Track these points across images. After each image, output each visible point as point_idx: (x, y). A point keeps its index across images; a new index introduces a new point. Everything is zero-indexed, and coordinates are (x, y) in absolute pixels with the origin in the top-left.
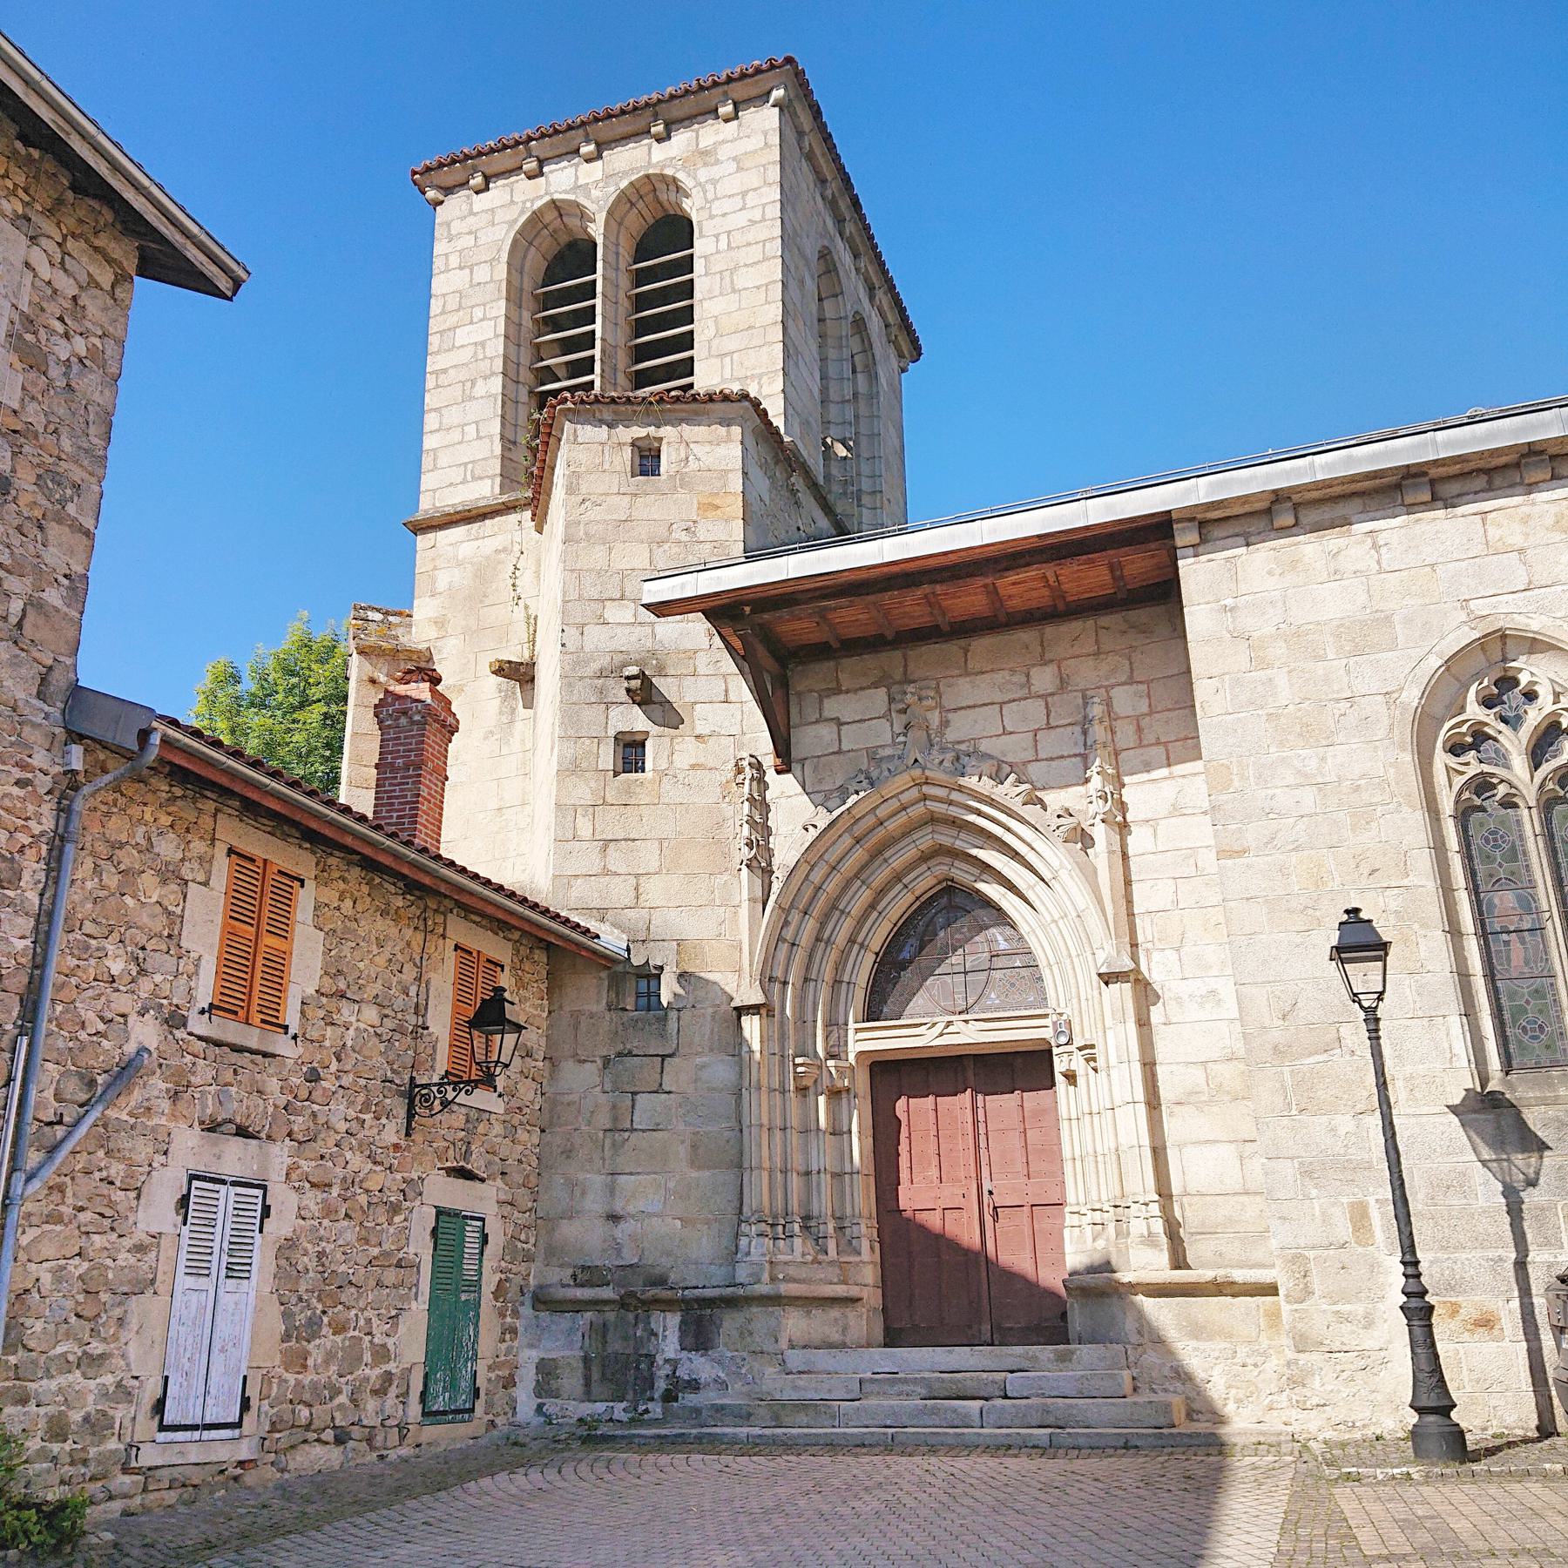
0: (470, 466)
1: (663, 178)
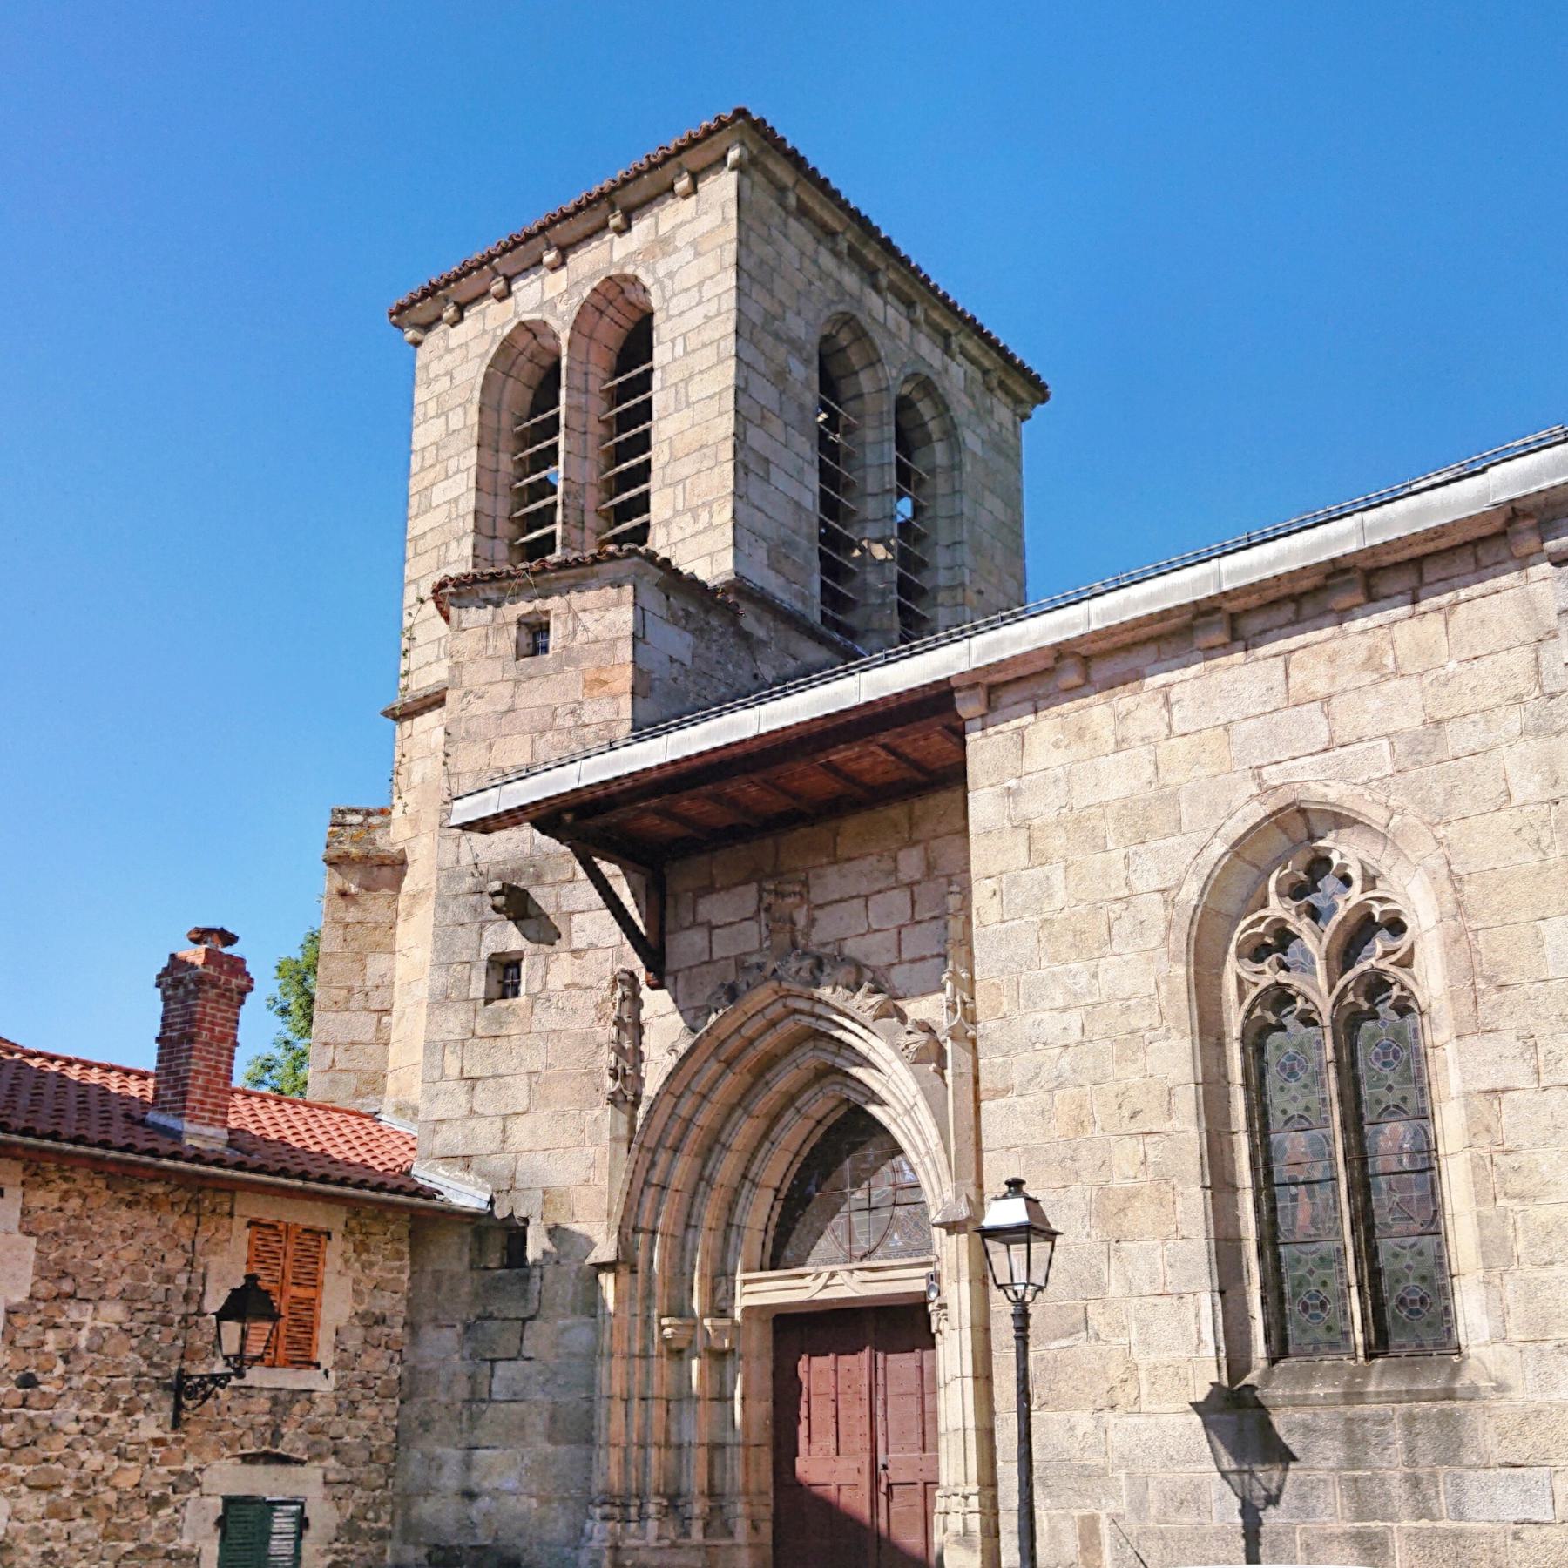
1: (625, 278)
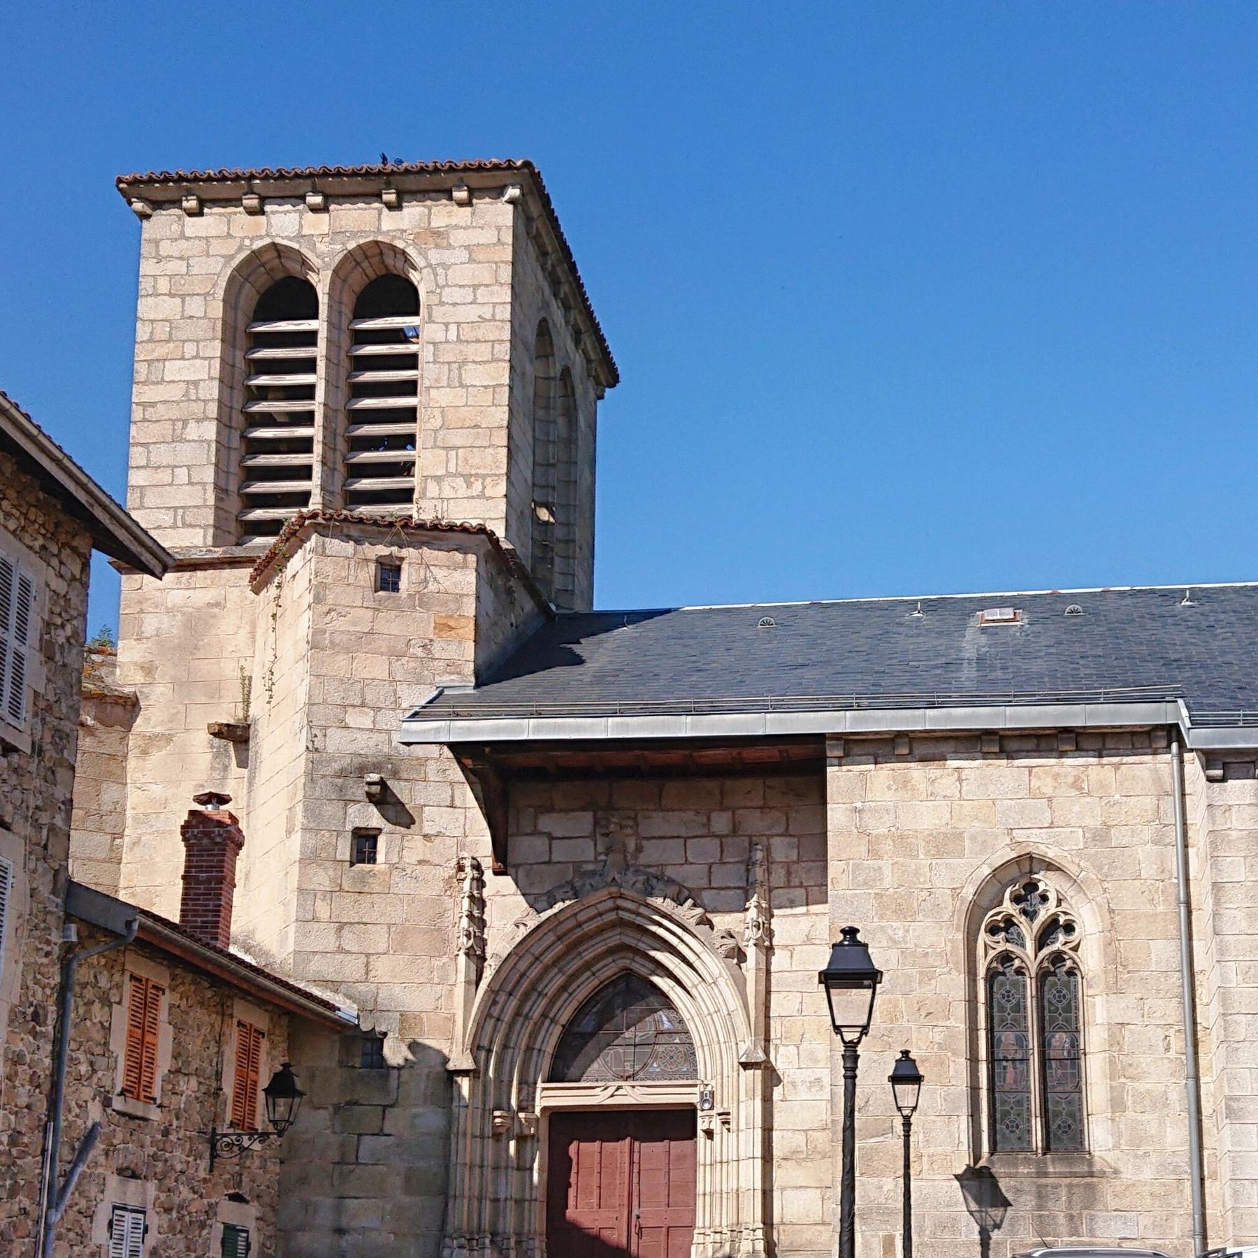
0: (180, 512)
